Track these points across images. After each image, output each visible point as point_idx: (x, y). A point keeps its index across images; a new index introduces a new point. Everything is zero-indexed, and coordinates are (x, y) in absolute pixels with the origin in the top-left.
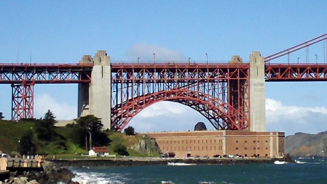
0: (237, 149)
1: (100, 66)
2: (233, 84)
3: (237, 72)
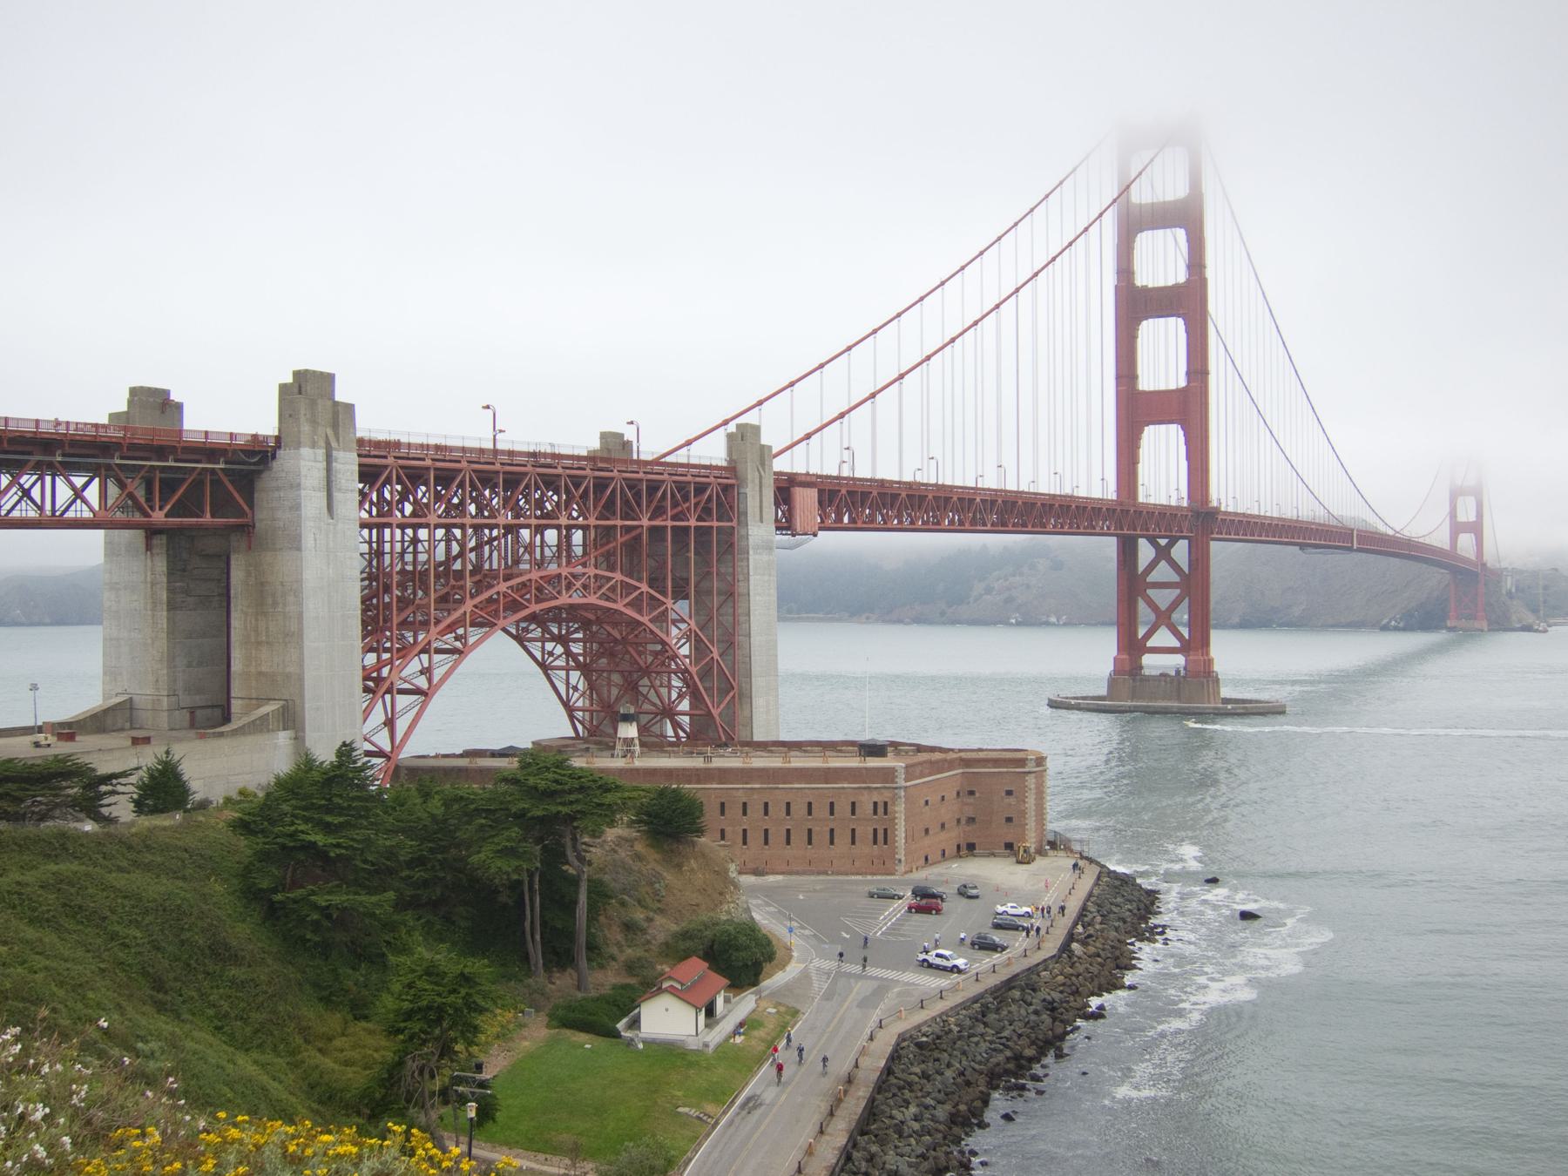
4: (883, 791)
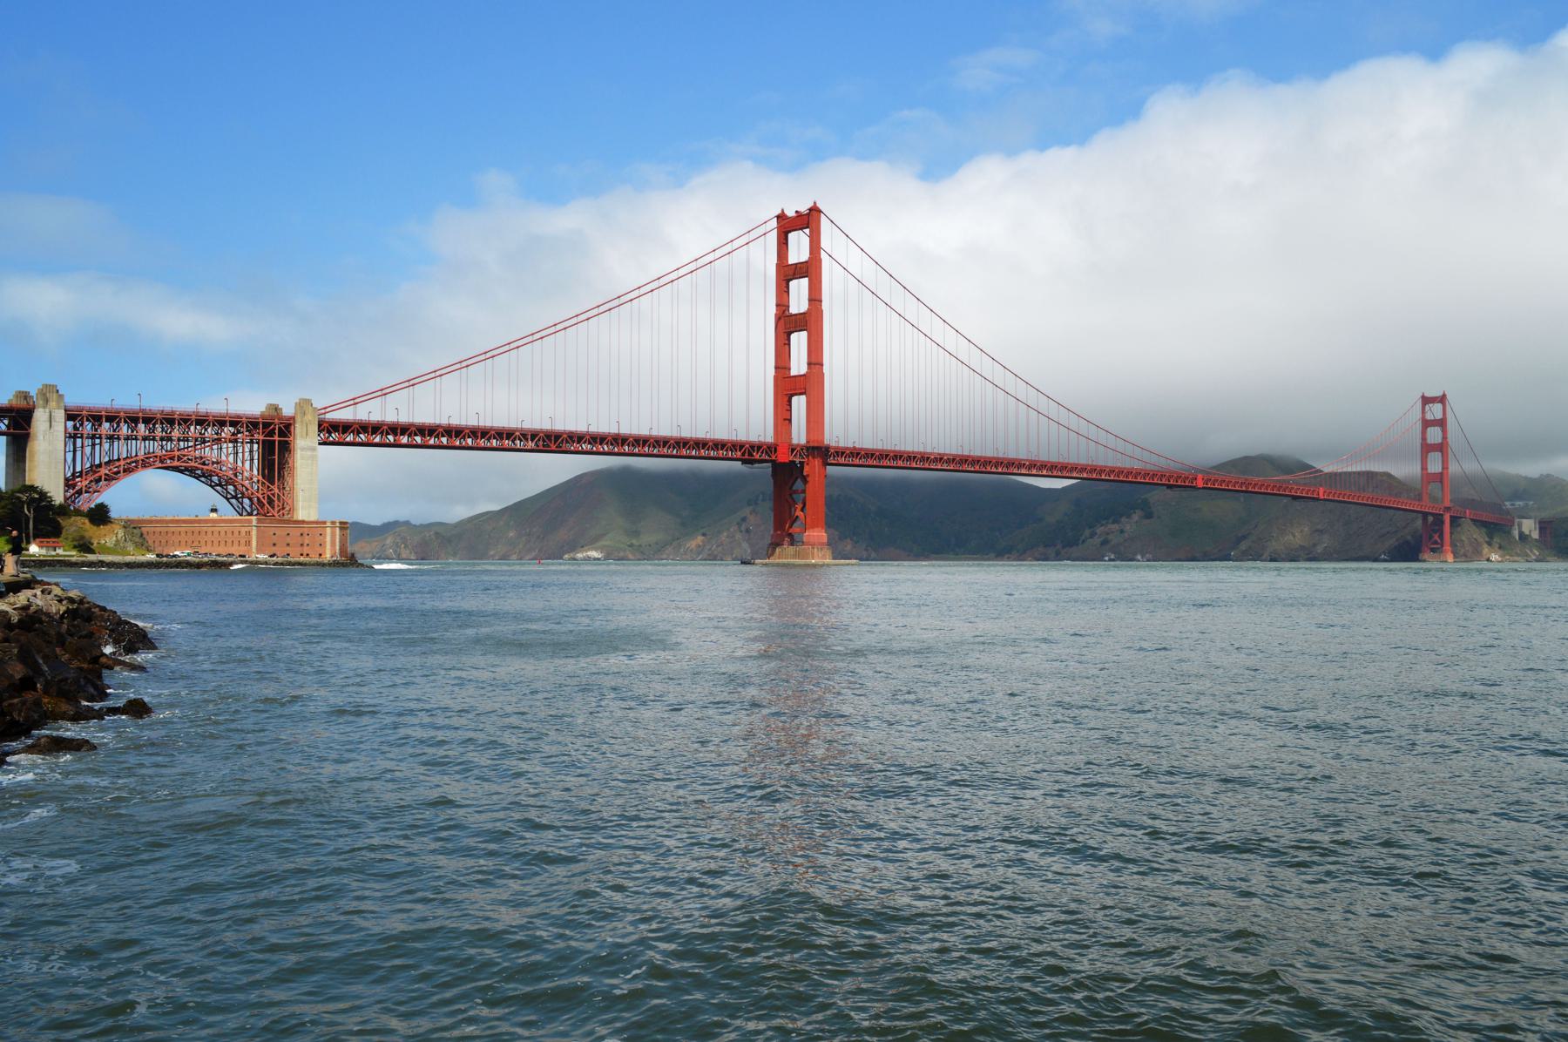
1: (47, 410)
2: (268, 448)
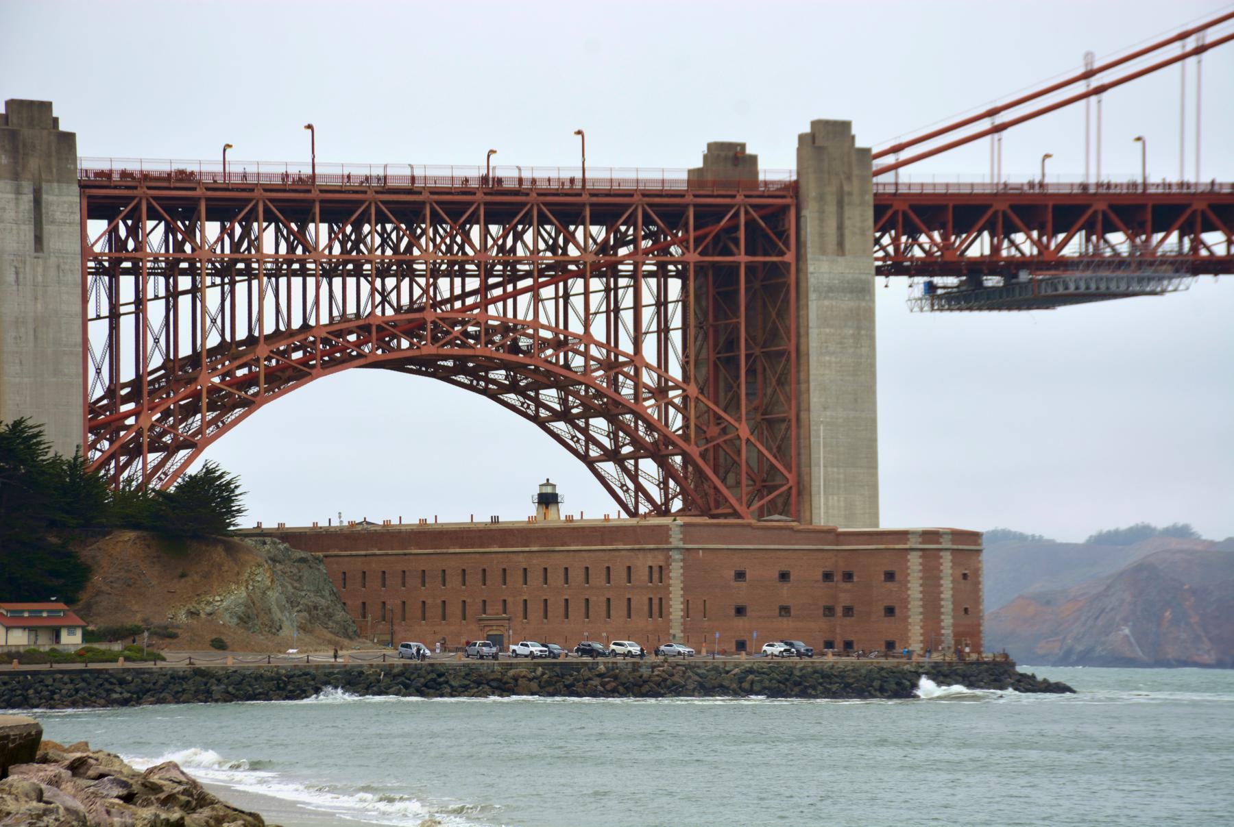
0: (740, 611)
3: (736, 228)
4: (656, 553)
